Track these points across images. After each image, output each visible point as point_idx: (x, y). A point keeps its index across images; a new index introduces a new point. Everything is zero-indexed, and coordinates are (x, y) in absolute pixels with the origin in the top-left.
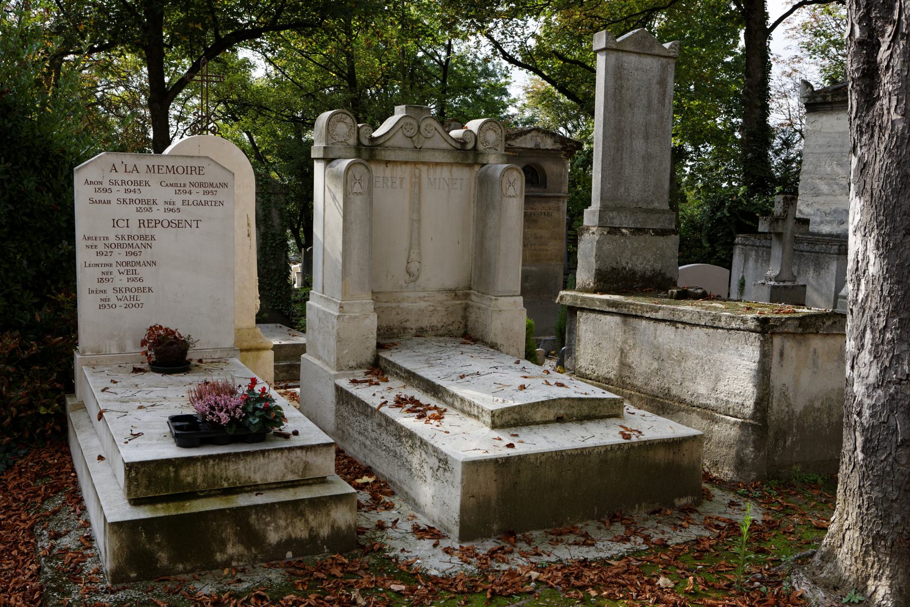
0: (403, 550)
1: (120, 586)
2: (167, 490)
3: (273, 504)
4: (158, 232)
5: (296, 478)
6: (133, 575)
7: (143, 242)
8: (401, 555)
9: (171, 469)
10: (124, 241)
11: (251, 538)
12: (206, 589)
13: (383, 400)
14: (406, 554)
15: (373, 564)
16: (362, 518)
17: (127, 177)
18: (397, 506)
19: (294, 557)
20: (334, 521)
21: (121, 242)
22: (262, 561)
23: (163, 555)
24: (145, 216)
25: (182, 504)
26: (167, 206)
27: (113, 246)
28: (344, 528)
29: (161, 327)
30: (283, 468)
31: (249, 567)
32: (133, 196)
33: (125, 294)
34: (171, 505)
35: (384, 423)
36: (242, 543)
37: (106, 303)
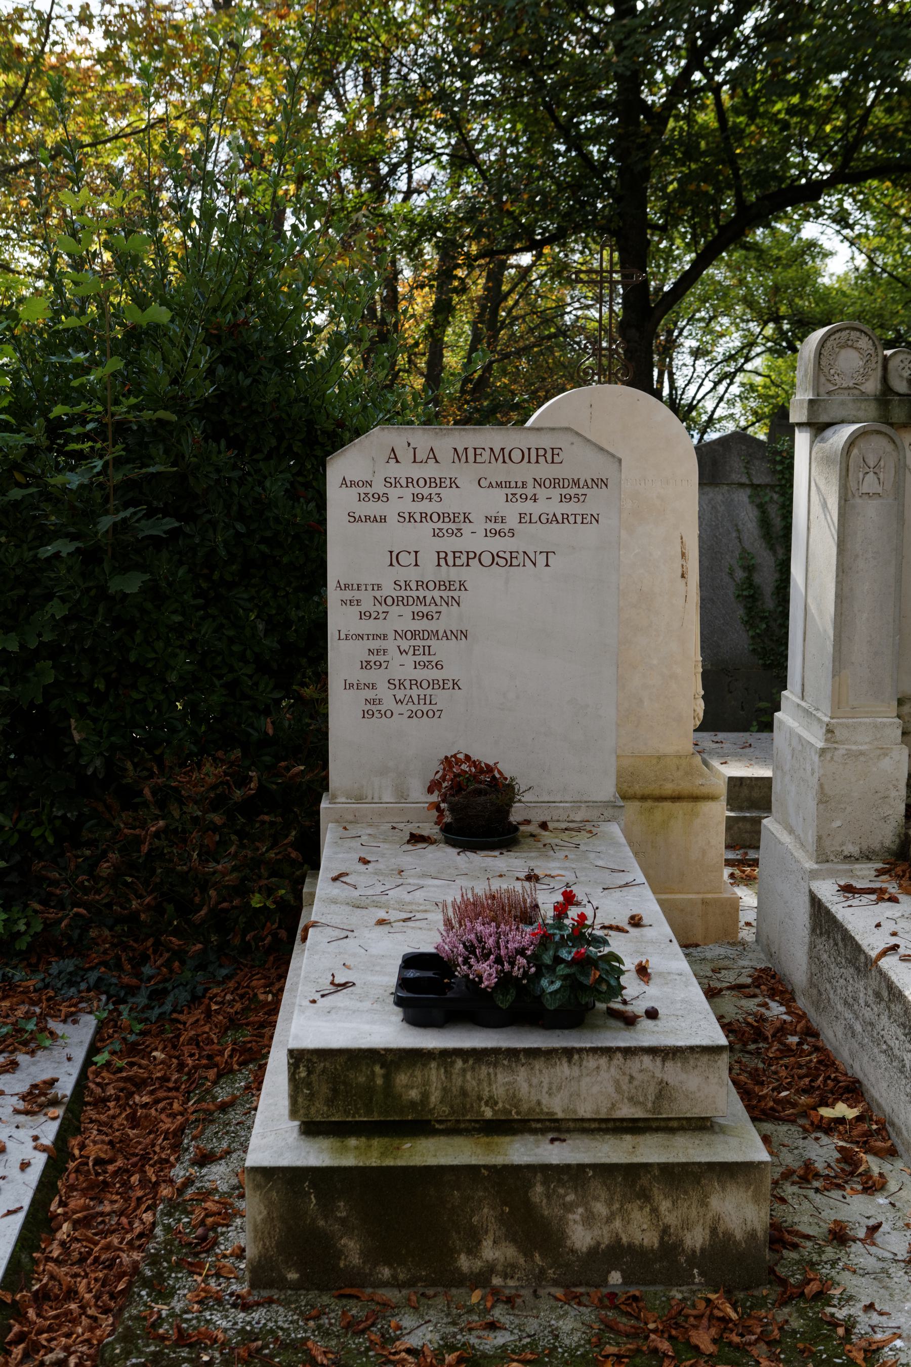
0: (870, 1307)
1: (266, 1293)
2: (369, 1112)
3: (582, 1167)
4: (472, 574)
5: (639, 1114)
6: (293, 1276)
7: (445, 594)
8: (863, 1318)
9: (377, 1069)
10: (409, 593)
11: (536, 1234)
12: (421, 1333)
13: (893, 941)
14: (875, 1318)
15: (794, 1332)
16: (806, 1205)
17: (416, 472)
18: (893, 1186)
19: (625, 1283)
20: (717, 1219)
21: (404, 593)
22: (556, 1283)
23: (351, 1244)
24: (449, 544)
25: (396, 1142)
26: (489, 526)
27: (389, 601)
28: (739, 1235)
29: (467, 757)
30: (611, 1090)
31: (526, 1293)
32: (427, 507)
33: (409, 692)
34: (375, 1142)
35: (885, 994)
36: (514, 1241)
37: (374, 708)
